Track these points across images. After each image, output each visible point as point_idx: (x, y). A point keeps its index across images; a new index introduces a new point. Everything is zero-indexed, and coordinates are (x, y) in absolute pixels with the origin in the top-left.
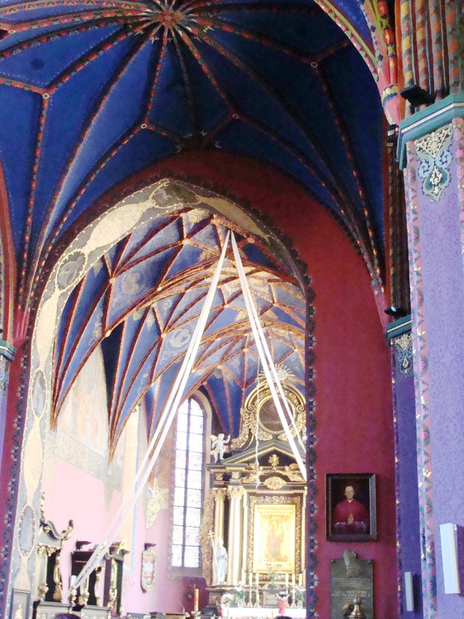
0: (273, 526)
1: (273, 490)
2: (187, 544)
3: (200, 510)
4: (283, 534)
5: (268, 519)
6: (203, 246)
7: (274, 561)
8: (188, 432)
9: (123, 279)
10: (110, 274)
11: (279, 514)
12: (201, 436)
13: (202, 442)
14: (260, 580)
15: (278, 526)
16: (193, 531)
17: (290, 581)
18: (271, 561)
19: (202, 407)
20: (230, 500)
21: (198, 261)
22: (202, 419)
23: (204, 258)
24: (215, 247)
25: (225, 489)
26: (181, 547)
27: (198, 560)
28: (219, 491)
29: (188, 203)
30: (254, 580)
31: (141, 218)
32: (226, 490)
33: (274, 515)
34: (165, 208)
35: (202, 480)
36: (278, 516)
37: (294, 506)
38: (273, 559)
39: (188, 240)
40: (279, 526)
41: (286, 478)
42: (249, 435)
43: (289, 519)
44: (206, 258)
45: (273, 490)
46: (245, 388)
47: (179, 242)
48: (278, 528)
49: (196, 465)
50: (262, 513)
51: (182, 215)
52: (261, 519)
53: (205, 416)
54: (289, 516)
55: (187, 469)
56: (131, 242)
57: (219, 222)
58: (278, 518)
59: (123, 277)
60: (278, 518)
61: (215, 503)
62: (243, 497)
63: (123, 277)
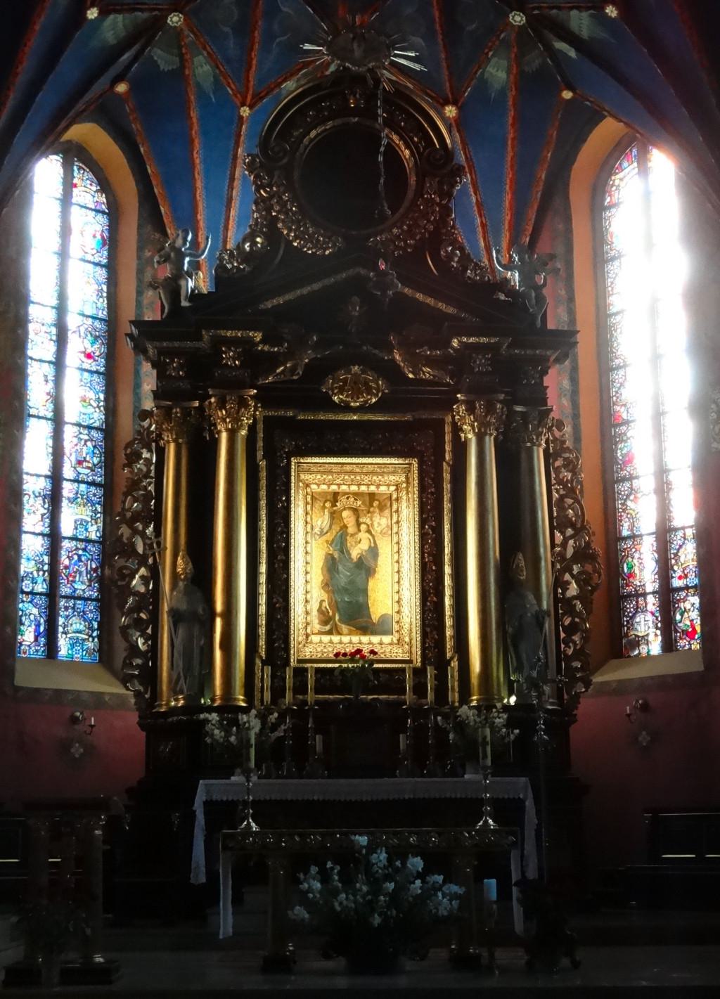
0: (345, 527)
1: (346, 408)
2: (65, 590)
3: (100, 492)
4: (374, 551)
5: (328, 505)
7: (349, 634)
8: (63, 254)
11: (363, 488)
12: (102, 274)
13: (105, 288)
14: (318, 690)
15: (358, 524)
16: (80, 552)
17: (420, 689)
18: (339, 633)
19: (105, 185)
20: (215, 443)
22: (103, 220)
25: (197, 404)
26: (42, 601)
27: (96, 640)
28: (177, 411)
30: (300, 688)
32: (201, 409)
33: (345, 494)
35: (106, 400)
36: (357, 495)
37: (415, 462)
38: (344, 628)
40: (363, 527)
41: (391, 373)
42: (267, 237)
43: (395, 507)
45: (346, 408)
46: (251, 107)
48: (360, 531)
49: (89, 356)
50: (307, 486)
52: (307, 503)
53: (113, 213)
54: (395, 496)
55: (59, 364)
58: (359, 503)
60: (359, 503)
61: (161, 453)
62: (252, 429)
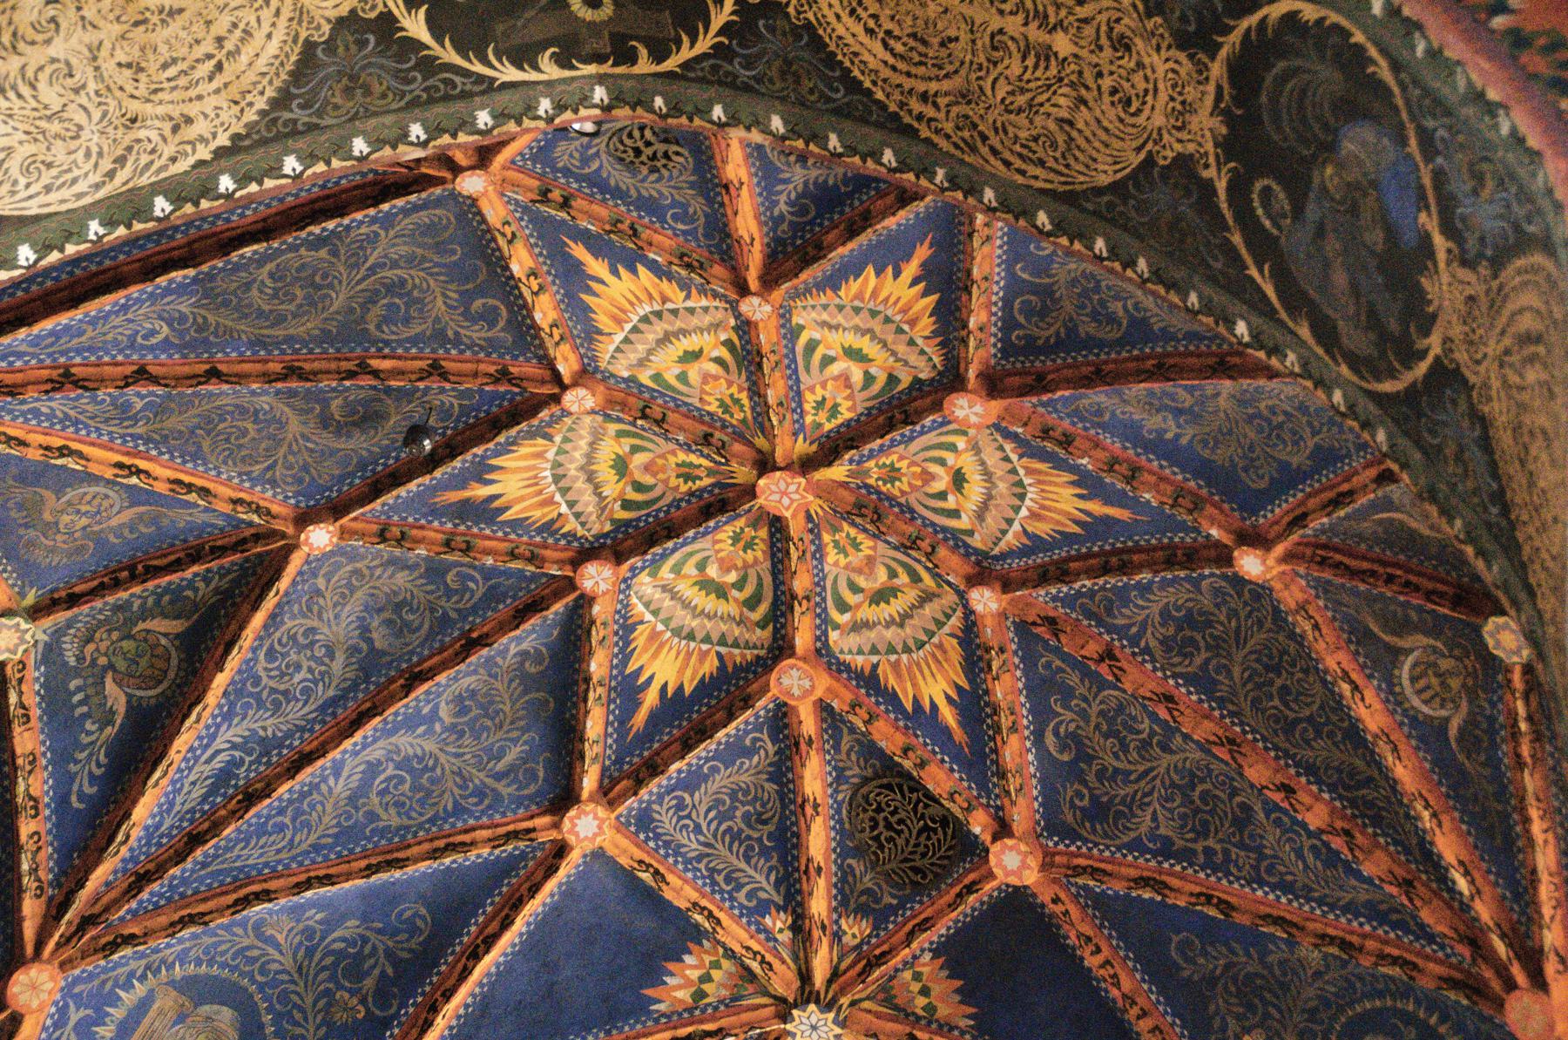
6: (694, 896)
9: (117, 1013)
10: (29, 930)
21: (641, 1008)
23: (684, 995)
24: (768, 920)
29: (644, 66)
31: (281, 101)
34: (479, 68)
39: (601, 812)
44: (700, 994)
47: (546, 820)
51: (596, 577)
56: (228, 717)
57: (819, 693)
59: (114, 1000)
63: (114, 1000)
